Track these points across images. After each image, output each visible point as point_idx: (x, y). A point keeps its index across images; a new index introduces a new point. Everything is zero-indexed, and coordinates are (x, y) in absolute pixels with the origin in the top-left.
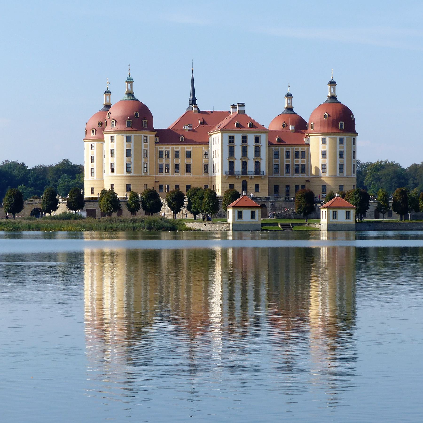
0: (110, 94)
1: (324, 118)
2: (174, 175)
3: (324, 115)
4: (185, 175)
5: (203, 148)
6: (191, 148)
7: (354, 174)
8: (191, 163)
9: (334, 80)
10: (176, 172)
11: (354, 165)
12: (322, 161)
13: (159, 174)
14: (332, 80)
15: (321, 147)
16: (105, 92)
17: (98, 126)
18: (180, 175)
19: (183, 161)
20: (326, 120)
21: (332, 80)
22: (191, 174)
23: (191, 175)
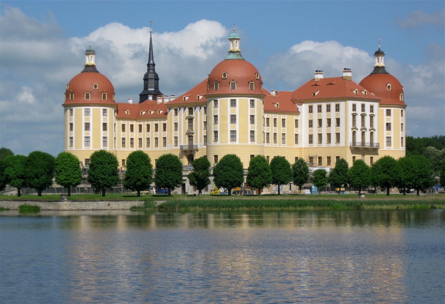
0: (94, 53)
1: (387, 89)
2: (273, 146)
3: (388, 85)
4: (282, 146)
5: (295, 117)
6: (286, 117)
7: (403, 147)
8: (286, 132)
9: (381, 50)
10: (274, 143)
11: (402, 138)
12: (387, 134)
13: (266, 144)
14: (379, 50)
15: (386, 119)
16: (87, 51)
17: (94, 88)
18: (277, 145)
19: (280, 130)
20: (389, 91)
21: (379, 50)
22: (286, 145)
23: (286, 146)
